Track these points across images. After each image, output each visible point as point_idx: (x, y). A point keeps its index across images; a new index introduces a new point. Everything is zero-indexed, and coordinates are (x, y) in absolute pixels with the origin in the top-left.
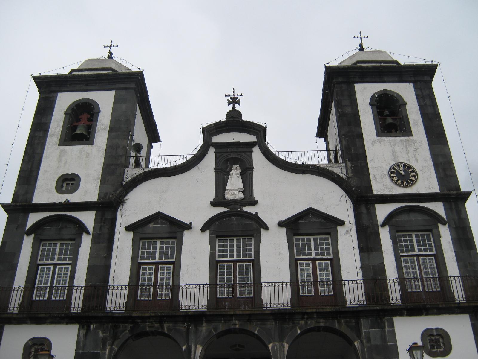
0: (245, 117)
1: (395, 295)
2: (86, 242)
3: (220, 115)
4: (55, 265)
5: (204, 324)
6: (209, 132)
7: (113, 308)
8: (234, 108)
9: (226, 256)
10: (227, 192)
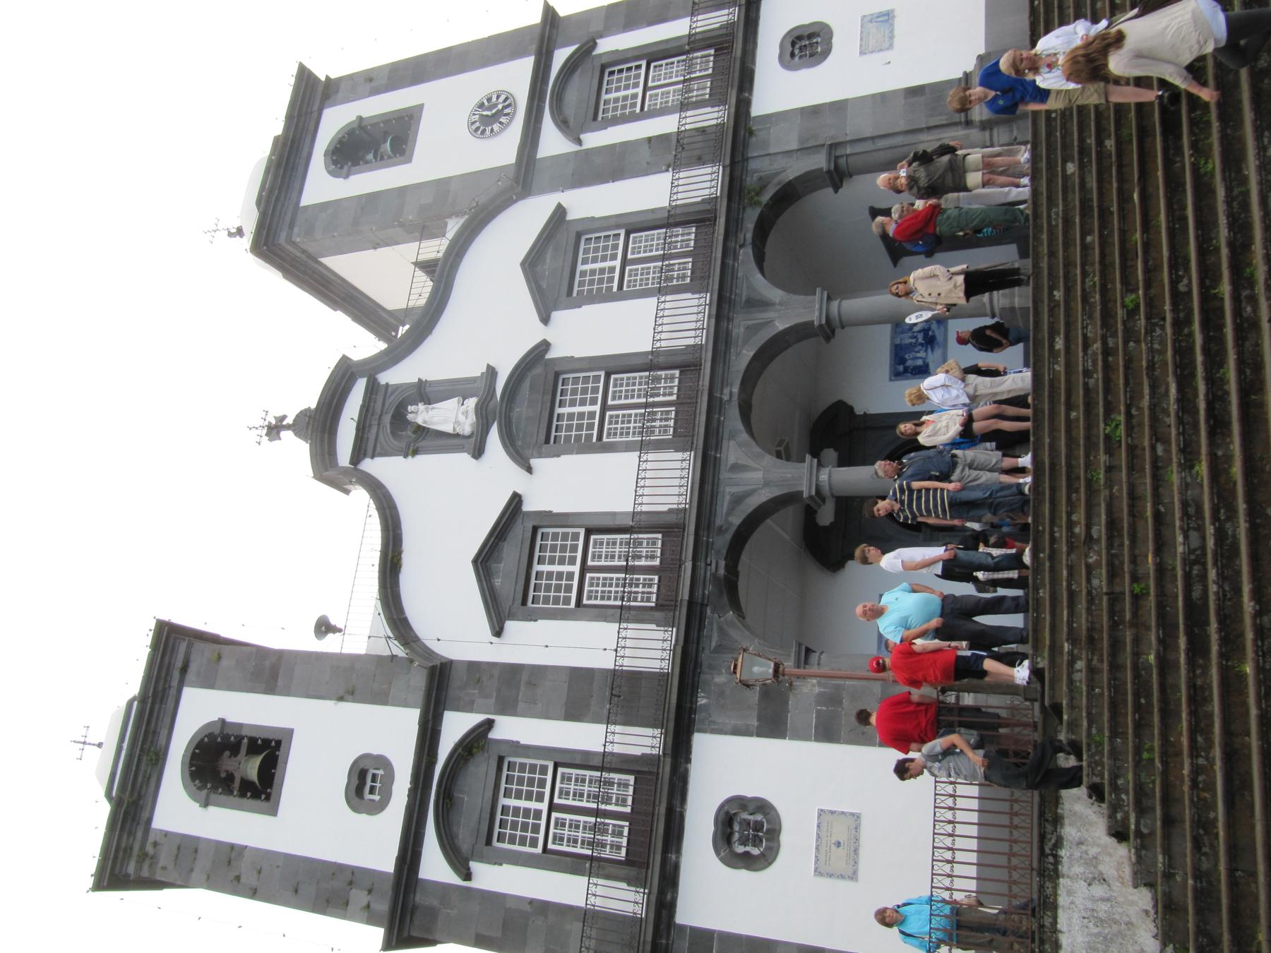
0: (311, 400)
1: (711, 117)
2: (509, 728)
3: (296, 450)
6: (324, 466)
8: (288, 427)
10: (459, 430)
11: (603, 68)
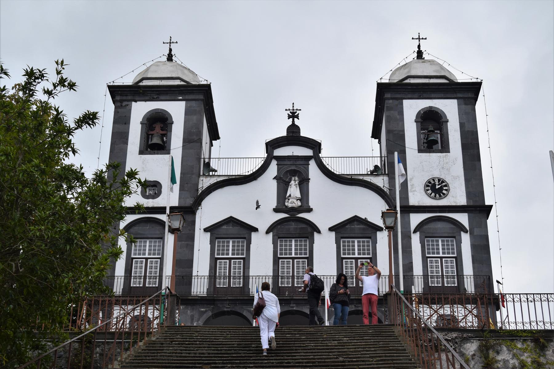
4: (147, 259)
6: (272, 145)
7: (198, 293)
9: (286, 254)
11: (454, 237)
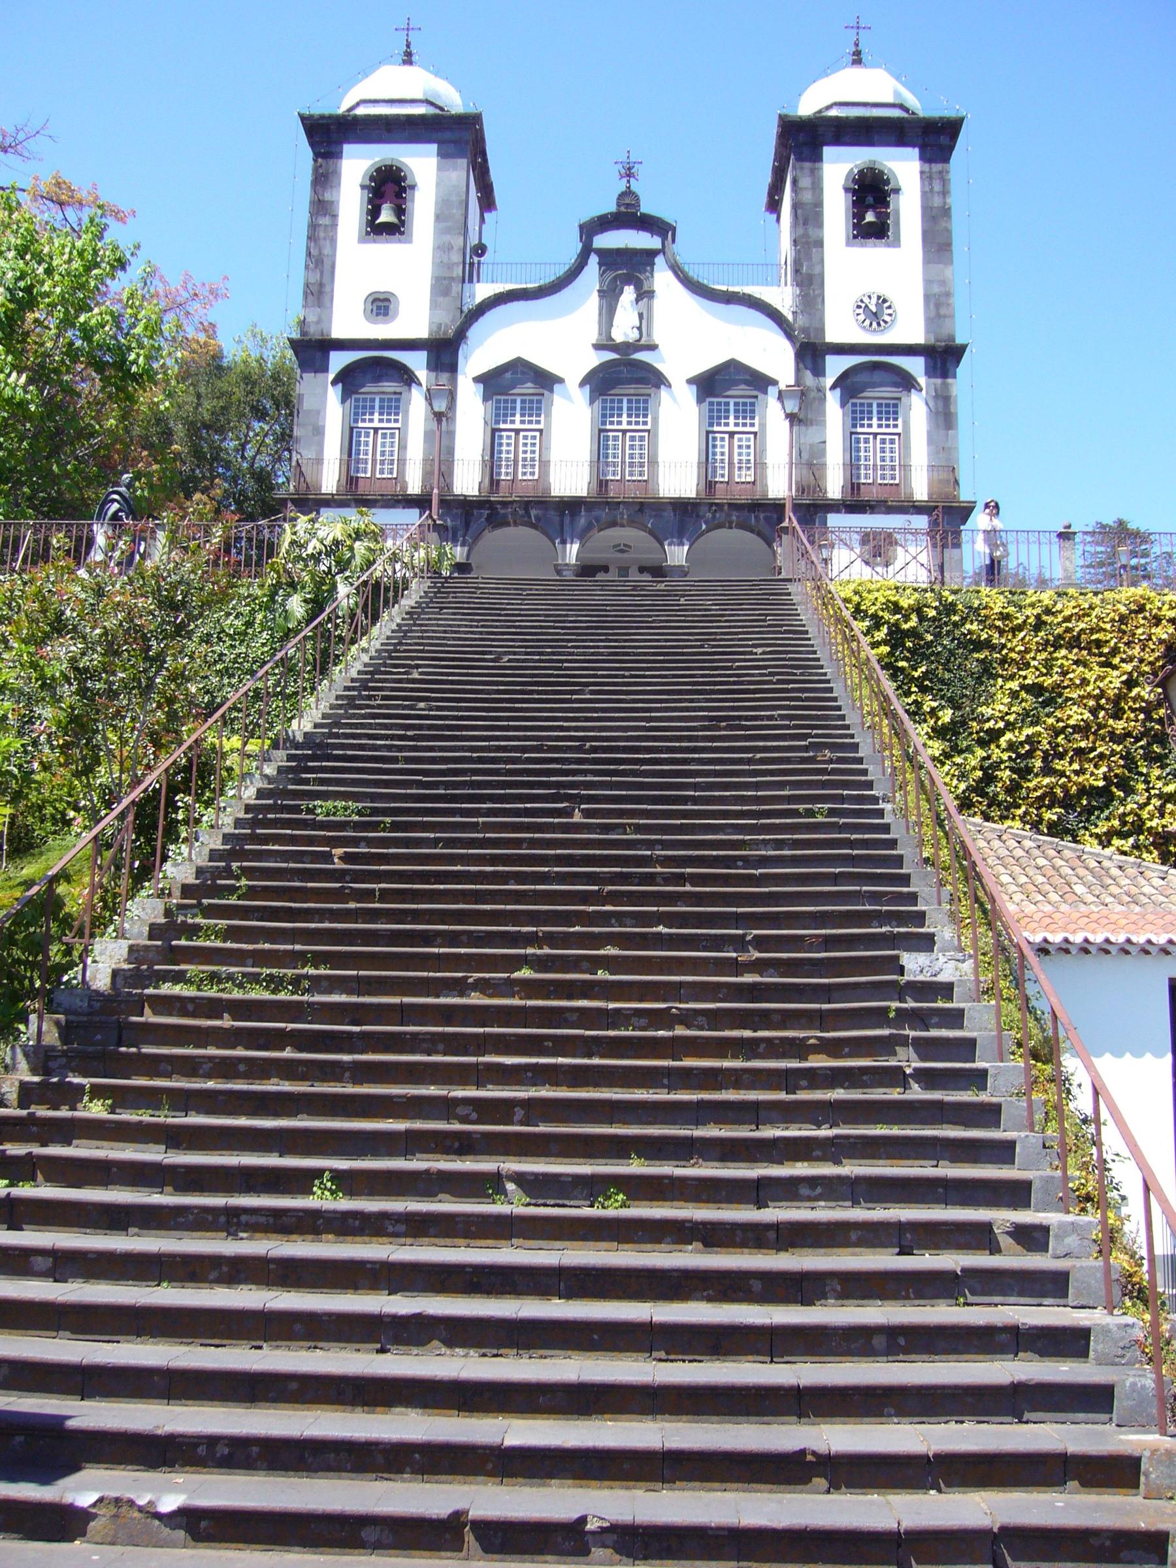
1: (834, 488)
5: (583, 513)
6: (590, 229)
